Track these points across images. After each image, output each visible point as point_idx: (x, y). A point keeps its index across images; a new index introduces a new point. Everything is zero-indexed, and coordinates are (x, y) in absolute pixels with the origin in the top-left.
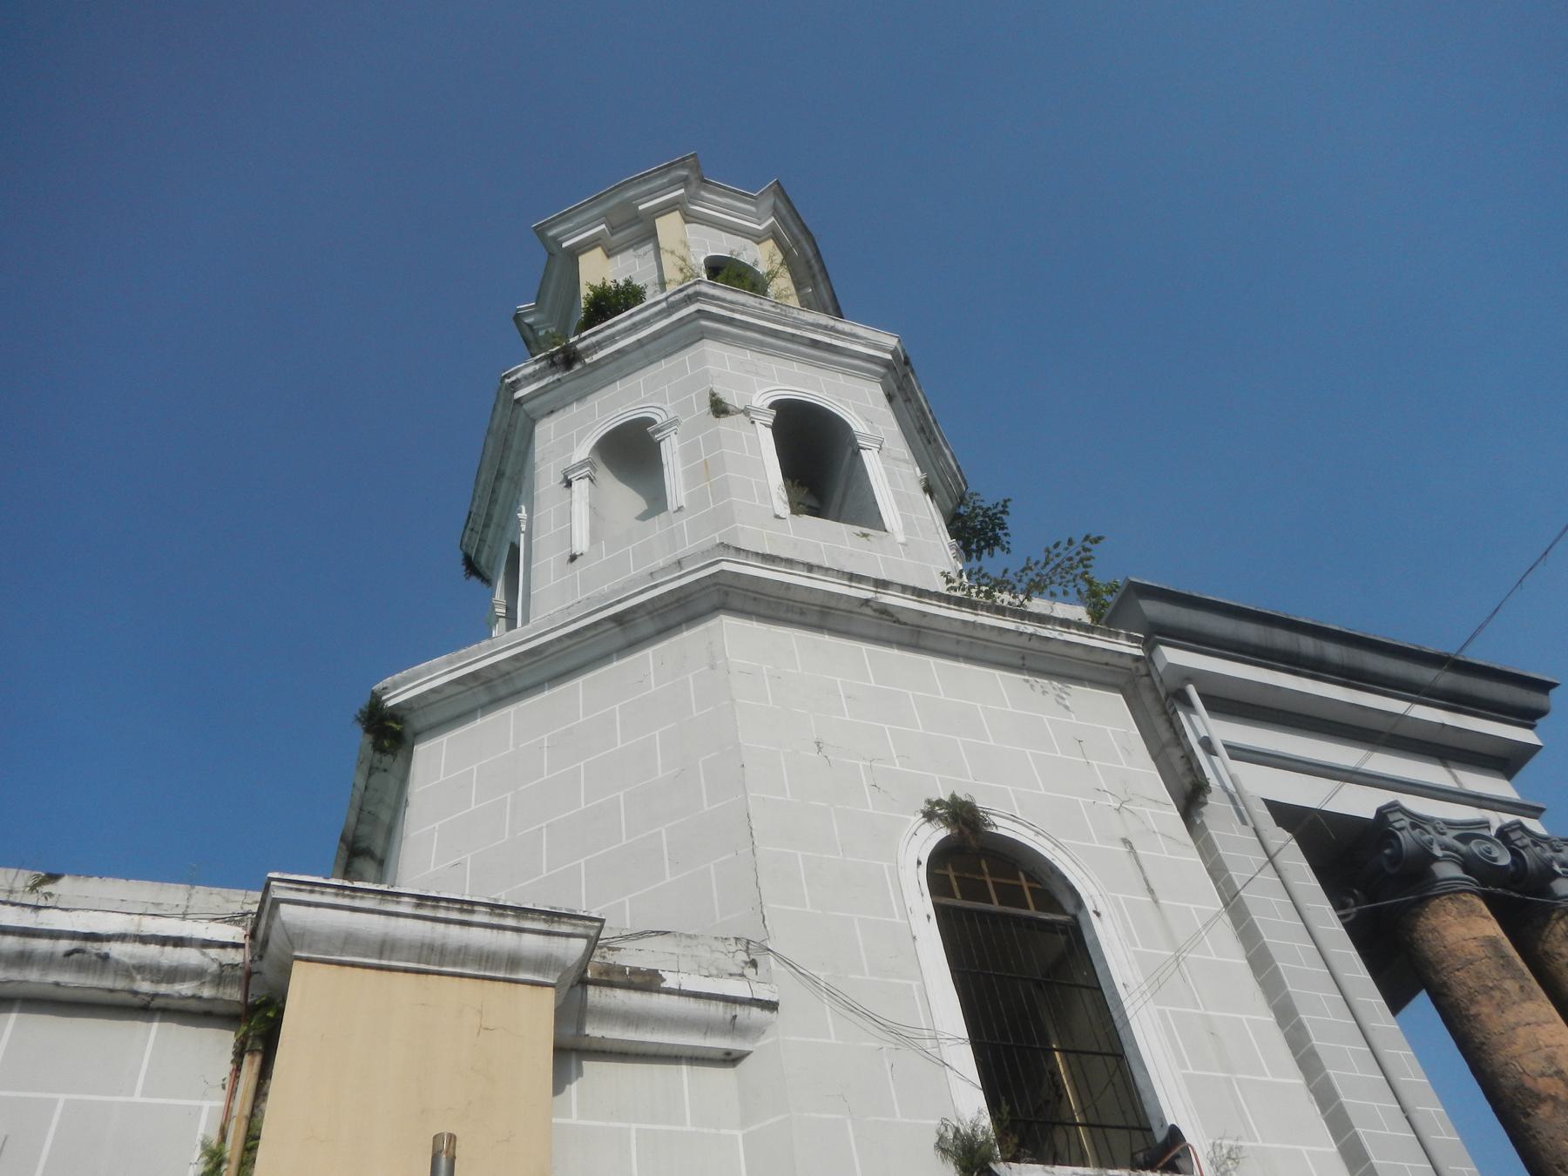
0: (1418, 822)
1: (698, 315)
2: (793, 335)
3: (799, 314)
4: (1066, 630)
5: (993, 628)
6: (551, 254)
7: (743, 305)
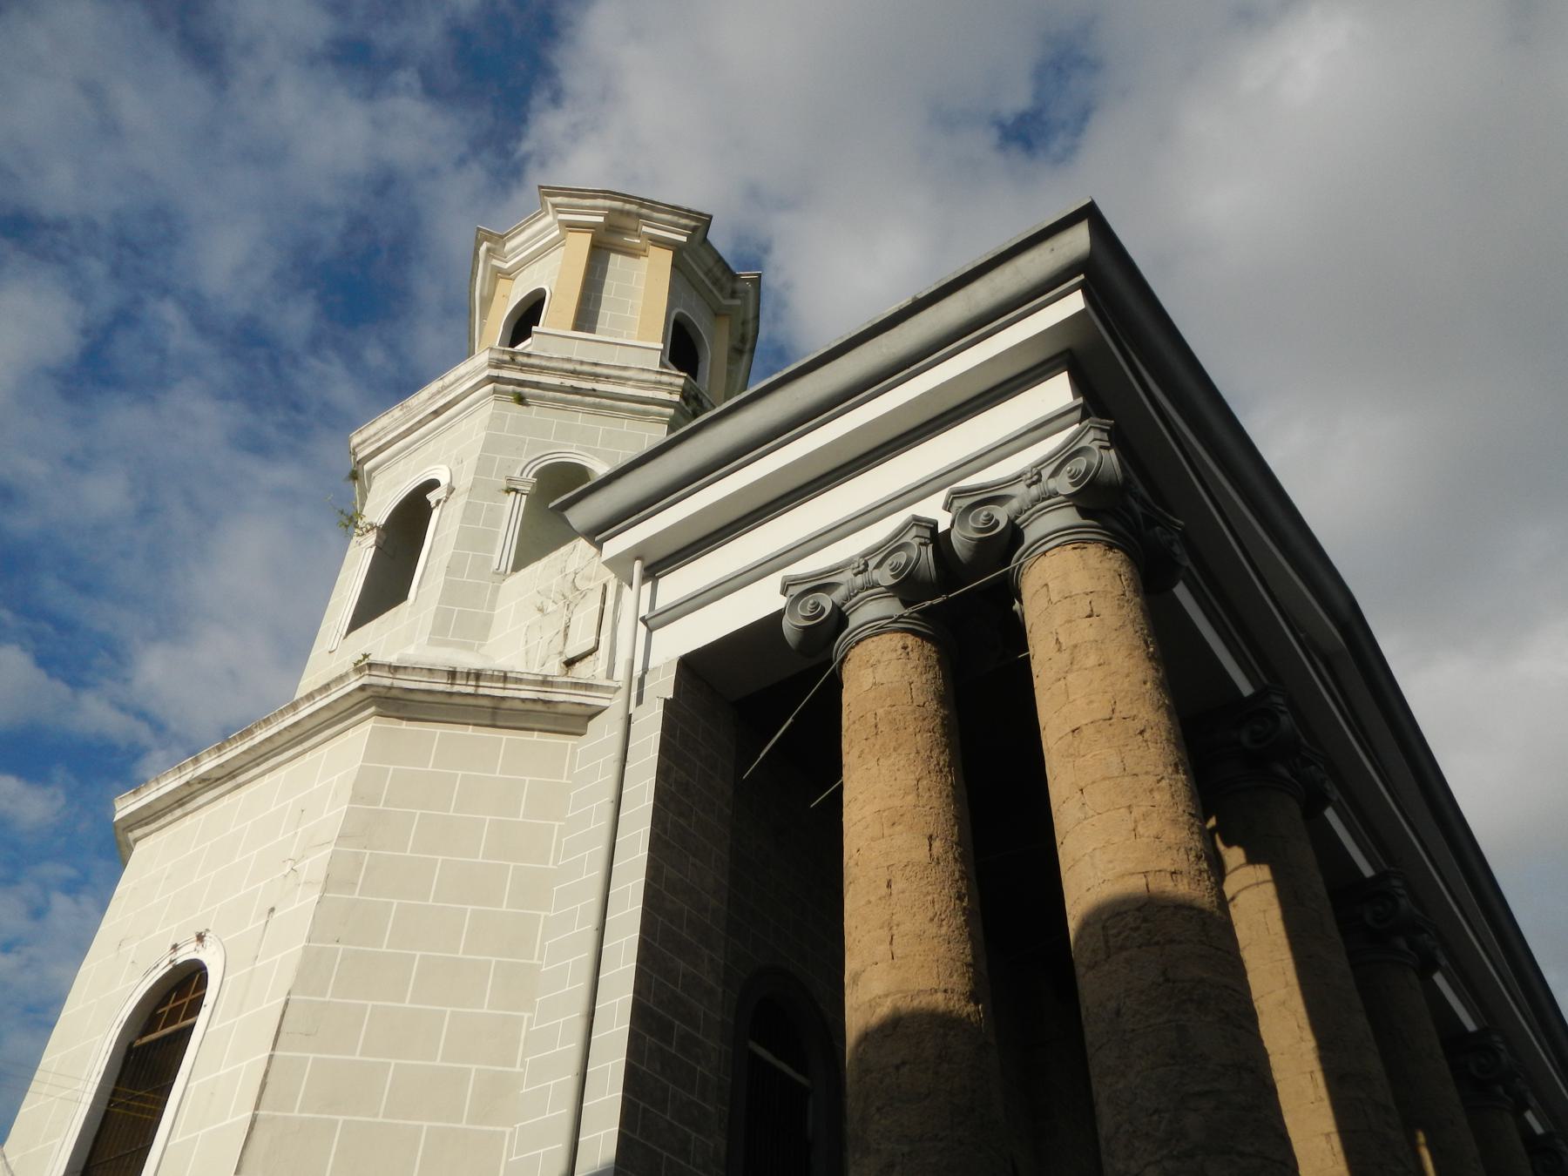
0: (821, 584)
2: (419, 422)
5: (262, 743)
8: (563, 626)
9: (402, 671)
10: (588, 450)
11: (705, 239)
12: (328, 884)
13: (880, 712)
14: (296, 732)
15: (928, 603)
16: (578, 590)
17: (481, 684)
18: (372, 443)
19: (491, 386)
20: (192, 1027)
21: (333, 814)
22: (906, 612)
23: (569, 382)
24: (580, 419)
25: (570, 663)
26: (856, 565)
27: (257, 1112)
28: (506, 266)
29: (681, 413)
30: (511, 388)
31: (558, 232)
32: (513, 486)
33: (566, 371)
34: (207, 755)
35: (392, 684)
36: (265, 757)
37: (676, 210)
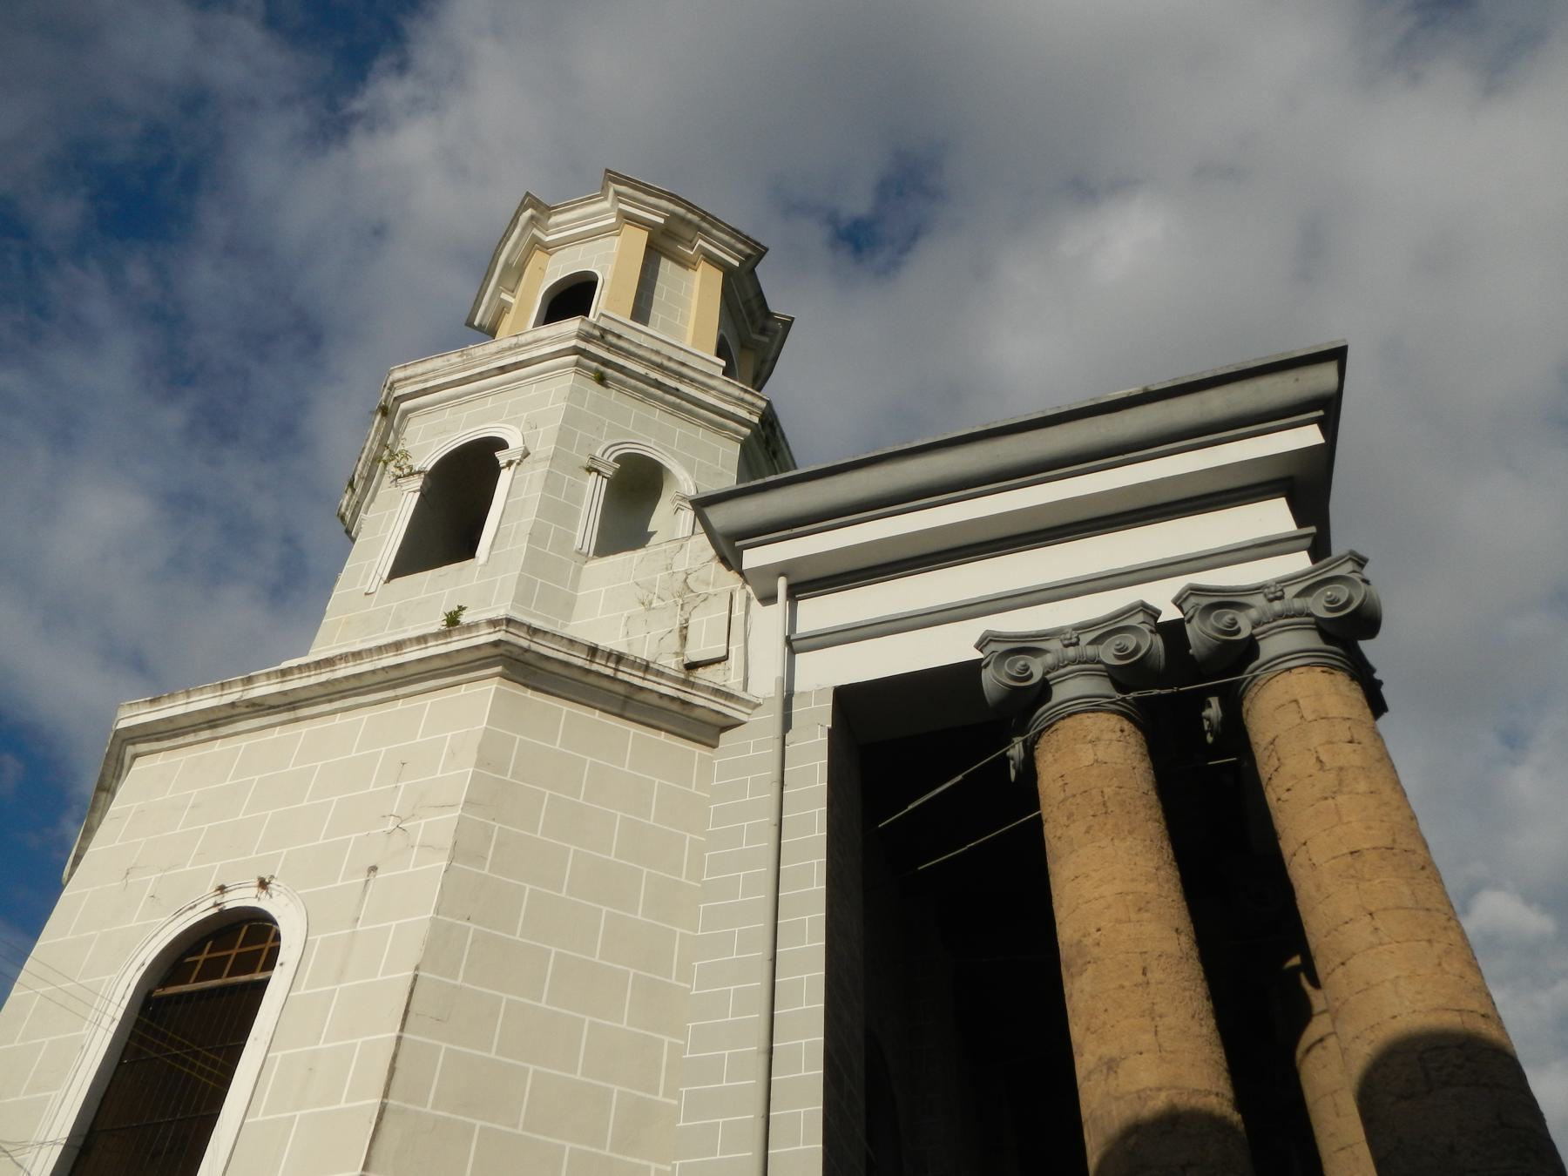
0: (1026, 646)
1: (396, 403)
3: (483, 350)
4: (423, 646)
5: (347, 678)
8: (677, 626)
9: (541, 635)
10: (665, 448)
11: (752, 271)
12: (457, 852)
13: (1108, 791)
15: (1156, 692)
16: (692, 591)
17: (621, 668)
18: (416, 383)
19: (574, 358)
20: (263, 985)
21: (457, 776)
22: (1119, 696)
23: (654, 375)
24: (657, 415)
25: (692, 666)
26: (1068, 636)
27: (386, 1101)
28: (548, 239)
29: (755, 436)
30: (594, 365)
31: (614, 220)
32: (595, 466)
33: (653, 363)
34: (264, 677)
35: (529, 646)
36: (343, 694)
37: (735, 233)
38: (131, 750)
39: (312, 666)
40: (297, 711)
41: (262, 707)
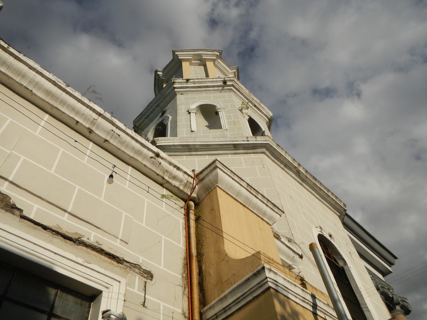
6: (173, 59)
7: (242, 89)
14: (325, 196)
38: (264, 150)
39: (312, 176)
40: (303, 183)
41: (298, 174)
